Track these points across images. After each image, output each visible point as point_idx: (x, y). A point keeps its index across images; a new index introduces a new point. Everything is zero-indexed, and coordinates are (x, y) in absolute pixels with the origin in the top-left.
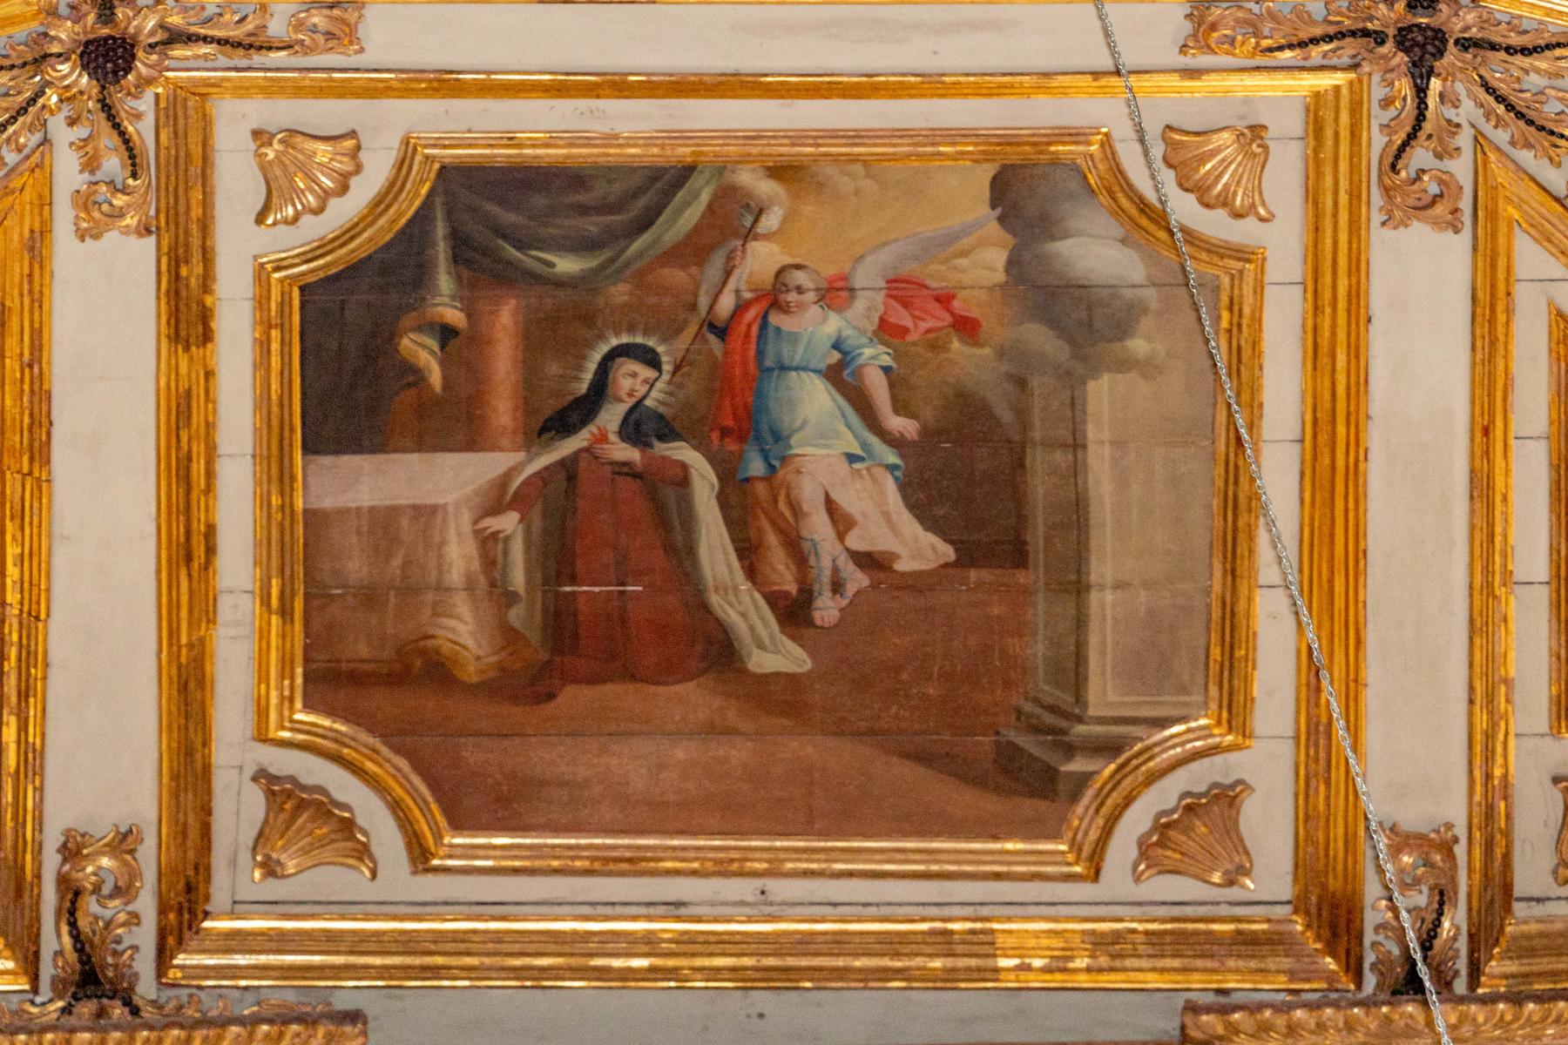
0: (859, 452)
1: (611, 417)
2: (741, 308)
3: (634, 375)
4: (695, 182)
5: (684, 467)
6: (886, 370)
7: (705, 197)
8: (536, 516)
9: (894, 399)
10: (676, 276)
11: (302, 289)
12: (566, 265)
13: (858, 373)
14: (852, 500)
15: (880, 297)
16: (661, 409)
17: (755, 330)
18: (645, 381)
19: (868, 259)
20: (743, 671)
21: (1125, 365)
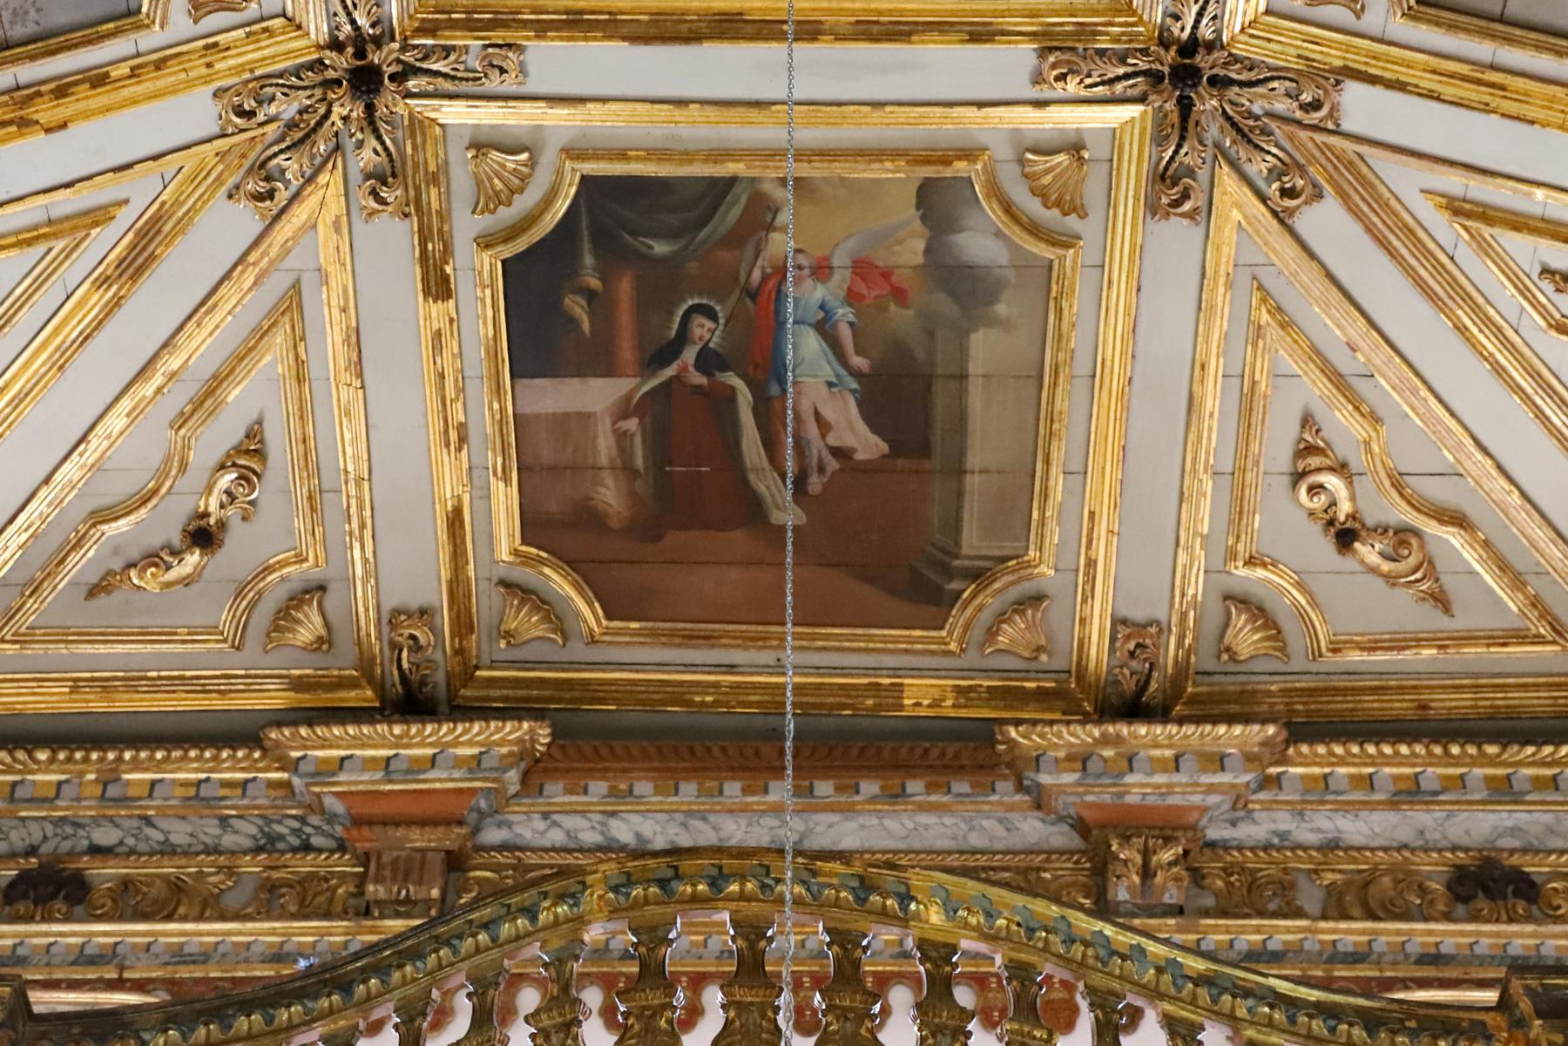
0: (834, 380)
1: (689, 355)
2: (765, 279)
3: (702, 326)
4: (737, 189)
5: (733, 389)
6: (851, 324)
7: (743, 200)
8: (648, 420)
9: (855, 344)
10: (724, 255)
11: (503, 262)
12: (660, 248)
13: (834, 326)
14: (828, 414)
15: (848, 273)
16: (719, 349)
17: (773, 294)
18: (709, 330)
19: (841, 246)
20: (769, 524)
21: (995, 322)
